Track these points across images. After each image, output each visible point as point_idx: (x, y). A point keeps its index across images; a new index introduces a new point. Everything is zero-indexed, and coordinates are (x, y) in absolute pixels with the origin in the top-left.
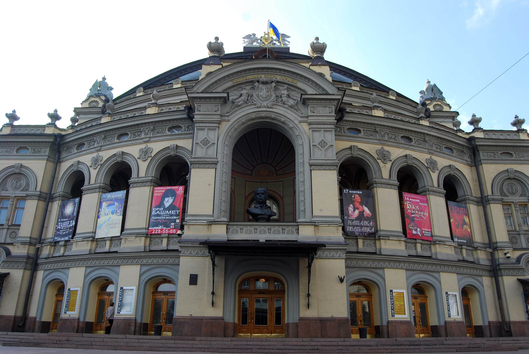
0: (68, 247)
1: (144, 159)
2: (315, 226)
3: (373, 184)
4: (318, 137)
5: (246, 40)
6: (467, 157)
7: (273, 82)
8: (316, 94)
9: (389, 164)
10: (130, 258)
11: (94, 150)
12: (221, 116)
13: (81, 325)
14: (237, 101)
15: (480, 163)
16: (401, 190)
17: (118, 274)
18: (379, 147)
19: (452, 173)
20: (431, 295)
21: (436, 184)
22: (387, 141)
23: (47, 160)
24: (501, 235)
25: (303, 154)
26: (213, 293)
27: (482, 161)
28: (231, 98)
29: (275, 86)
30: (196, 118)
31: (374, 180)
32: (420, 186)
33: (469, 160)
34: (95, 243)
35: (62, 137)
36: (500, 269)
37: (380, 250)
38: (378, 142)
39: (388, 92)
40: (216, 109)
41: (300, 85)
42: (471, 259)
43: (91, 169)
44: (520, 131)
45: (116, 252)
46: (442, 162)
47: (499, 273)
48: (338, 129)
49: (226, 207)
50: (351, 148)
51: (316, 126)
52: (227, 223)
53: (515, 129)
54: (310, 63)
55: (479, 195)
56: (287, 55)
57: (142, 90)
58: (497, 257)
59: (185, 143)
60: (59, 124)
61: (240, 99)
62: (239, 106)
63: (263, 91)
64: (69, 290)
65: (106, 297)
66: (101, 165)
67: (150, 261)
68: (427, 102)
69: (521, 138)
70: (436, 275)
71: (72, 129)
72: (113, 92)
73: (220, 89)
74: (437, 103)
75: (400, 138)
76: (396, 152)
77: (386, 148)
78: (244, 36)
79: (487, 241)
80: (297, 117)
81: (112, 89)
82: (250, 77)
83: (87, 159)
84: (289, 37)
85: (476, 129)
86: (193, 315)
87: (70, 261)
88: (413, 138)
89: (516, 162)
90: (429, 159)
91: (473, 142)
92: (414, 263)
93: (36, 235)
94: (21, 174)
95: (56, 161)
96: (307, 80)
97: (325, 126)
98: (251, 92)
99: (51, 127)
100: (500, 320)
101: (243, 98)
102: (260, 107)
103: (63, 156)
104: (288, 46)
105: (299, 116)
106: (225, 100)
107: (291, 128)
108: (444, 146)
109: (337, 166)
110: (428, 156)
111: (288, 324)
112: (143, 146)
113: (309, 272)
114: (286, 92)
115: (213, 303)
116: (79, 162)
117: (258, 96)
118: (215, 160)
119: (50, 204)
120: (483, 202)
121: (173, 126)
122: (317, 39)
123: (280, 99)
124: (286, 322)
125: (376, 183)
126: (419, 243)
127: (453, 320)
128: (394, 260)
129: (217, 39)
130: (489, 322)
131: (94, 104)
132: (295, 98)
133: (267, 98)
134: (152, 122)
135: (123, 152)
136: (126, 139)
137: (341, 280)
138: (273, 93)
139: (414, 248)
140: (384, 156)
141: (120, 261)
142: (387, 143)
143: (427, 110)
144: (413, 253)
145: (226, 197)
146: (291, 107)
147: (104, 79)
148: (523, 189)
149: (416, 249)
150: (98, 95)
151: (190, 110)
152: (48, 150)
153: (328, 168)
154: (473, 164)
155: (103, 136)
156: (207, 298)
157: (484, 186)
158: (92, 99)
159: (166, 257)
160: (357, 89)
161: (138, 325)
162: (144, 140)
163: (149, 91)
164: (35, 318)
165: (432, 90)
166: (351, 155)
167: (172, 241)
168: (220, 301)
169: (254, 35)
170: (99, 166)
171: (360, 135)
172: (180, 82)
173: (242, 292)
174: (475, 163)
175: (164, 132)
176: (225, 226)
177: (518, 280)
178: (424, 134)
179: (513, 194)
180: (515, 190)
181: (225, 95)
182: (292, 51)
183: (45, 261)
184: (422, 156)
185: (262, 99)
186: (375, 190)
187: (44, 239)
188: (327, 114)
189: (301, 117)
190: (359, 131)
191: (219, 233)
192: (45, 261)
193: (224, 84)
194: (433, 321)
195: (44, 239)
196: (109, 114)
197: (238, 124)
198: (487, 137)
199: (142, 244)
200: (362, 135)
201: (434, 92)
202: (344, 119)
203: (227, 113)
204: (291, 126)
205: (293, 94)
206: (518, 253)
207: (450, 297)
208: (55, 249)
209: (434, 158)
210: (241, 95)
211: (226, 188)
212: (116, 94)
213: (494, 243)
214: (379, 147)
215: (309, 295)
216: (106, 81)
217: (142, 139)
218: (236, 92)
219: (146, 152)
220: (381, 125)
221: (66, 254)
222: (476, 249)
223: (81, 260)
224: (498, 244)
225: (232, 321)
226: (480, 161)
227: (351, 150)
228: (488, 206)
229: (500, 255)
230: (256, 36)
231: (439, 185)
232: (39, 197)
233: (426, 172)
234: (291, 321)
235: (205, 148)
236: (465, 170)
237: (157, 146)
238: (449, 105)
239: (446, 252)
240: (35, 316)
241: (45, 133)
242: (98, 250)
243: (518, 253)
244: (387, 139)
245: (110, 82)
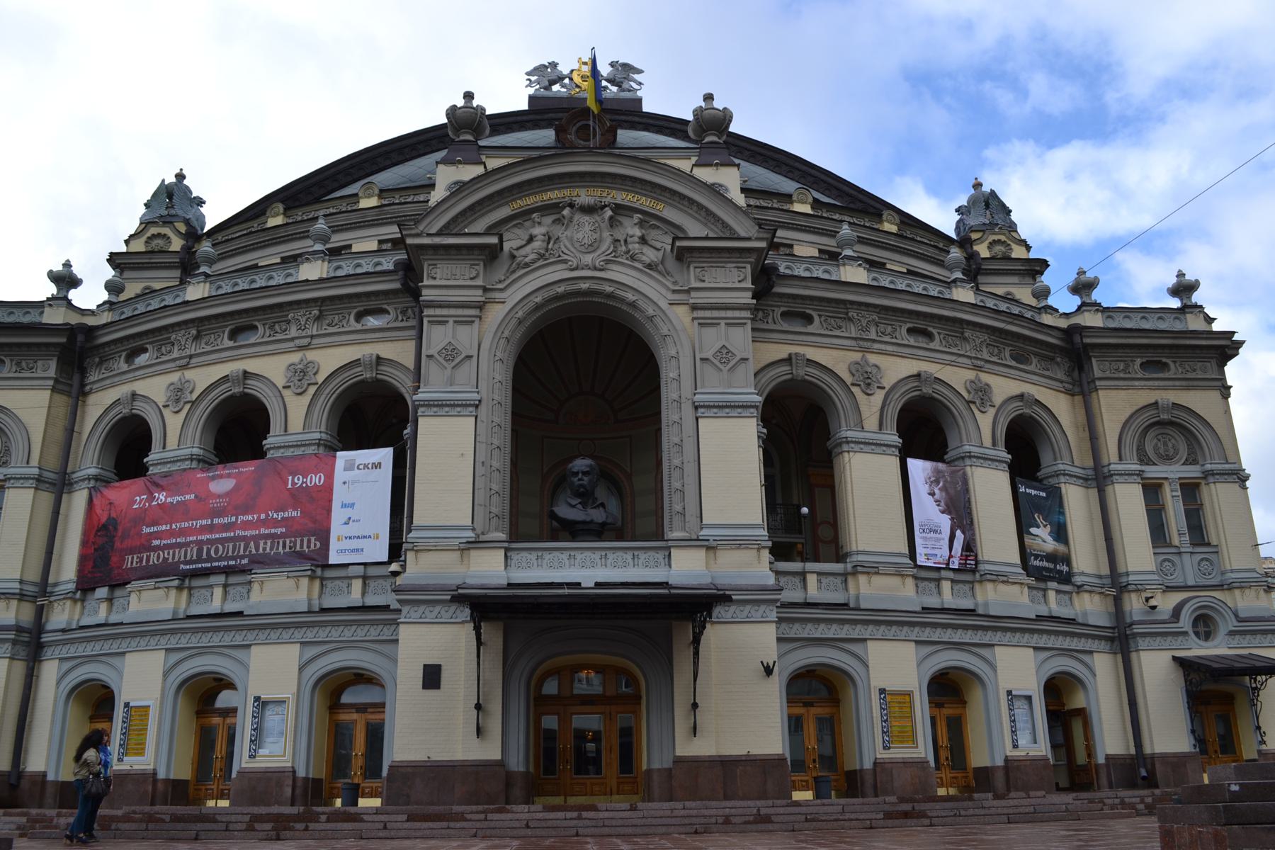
0: (116, 603)
1: (300, 391)
2: (708, 548)
3: (840, 444)
4: (712, 340)
5: (533, 78)
6: (1060, 375)
7: (605, 206)
8: (707, 238)
9: (879, 397)
10: (274, 627)
11: (172, 365)
12: (485, 290)
13: (160, 786)
14: (522, 252)
15: (1092, 386)
16: (905, 453)
17: (246, 667)
18: (857, 356)
19: (1027, 411)
20: (976, 698)
21: (987, 441)
22: (874, 341)
23: (54, 390)
24: (1138, 554)
25: (678, 380)
26: (478, 707)
27: (1098, 383)
28: (506, 246)
29: (611, 218)
30: (427, 294)
31: (843, 434)
32: (952, 443)
33: (1069, 380)
34: (185, 593)
35: (91, 331)
36: (1135, 635)
37: (857, 598)
38: (853, 343)
39: (880, 216)
40: (474, 274)
42: (1065, 612)
43: (166, 412)
45: (239, 614)
46: (1004, 387)
47: (1132, 644)
48: (760, 315)
49: (500, 505)
50: (788, 360)
51: (708, 314)
52: (506, 545)
53: (1175, 303)
54: (694, 159)
55: (1090, 463)
56: (637, 119)
57: (282, 210)
58: (1127, 608)
59: (400, 351)
60: (76, 296)
61: (528, 249)
62: (527, 265)
63: (584, 229)
64: (127, 705)
65: (216, 720)
66: (193, 403)
67: (322, 634)
68: (974, 236)
69: (1191, 328)
70: (984, 652)
71: (110, 310)
72: (204, 210)
73: (480, 226)
74: (996, 238)
75: (904, 331)
76: (896, 369)
77: (873, 359)
78: (530, 68)
79: (1105, 571)
80: (663, 291)
81: (201, 202)
82: (553, 195)
83: (155, 388)
84: (640, 72)
86: (433, 758)
87: (124, 636)
88: (935, 331)
89: (1177, 383)
90: (972, 382)
91: (1077, 339)
92: (935, 625)
93: (34, 575)
95: (75, 390)
96: (686, 203)
97: (730, 314)
98: (558, 231)
99: (59, 306)
100: (1133, 751)
101: (537, 244)
102: (576, 269)
103: (92, 379)
104: (639, 94)
105: (668, 289)
106: (491, 255)
107: (651, 318)
108: (1008, 349)
109: (756, 407)
110: (971, 375)
111: (649, 771)
112: (295, 358)
113: (696, 654)
115: (479, 731)
116: (134, 395)
117: (571, 240)
118: (475, 396)
119: (65, 496)
120: (1099, 479)
121: (368, 305)
122: (709, 97)
123: (624, 248)
124: (644, 767)
125: (848, 442)
126: (947, 579)
127: (1023, 754)
128: (888, 620)
129: (469, 96)
130: (1108, 757)
131: (159, 243)
132: (659, 245)
133: (592, 247)
134: (315, 300)
135: (245, 372)
136: (252, 340)
137: (768, 671)
138: (606, 234)
139: (935, 591)
140: (868, 380)
141: (251, 637)
142: (876, 346)
143: (972, 256)
144: (933, 602)
145: (500, 483)
146: (649, 266)
147: (180, 177)
148: (1190, 447)
149: (939, 593)
150: (167, 221)
151: (410, 273)
152: (53, 364)
153: (735, 412)
154: (1077, 389)
155: (194, 332)
156: (464, 716)
157: (1102, 440)
158: (153, 230)
159: (360, 623)
160: (806, 209)
161: (299, 784)
162: (298, 342)
163: (299, 215)
164: (44, 774)
165: (987, 206)
166: (789, 377)
167: (372, 584)
169: (554, 65)
170: (187, 407)
171: (810, 329)
172: (377, 192)
173: (539, 704)
174: (1081, 387)
175: (344, 322)
176: (502, 552)
177: (1174, 658)
178: (962, 321)
179: (1167, 459)
180: (1171, 452)
181: (494, 240)
182: (647, 108)
183: (60, 637)
185: (583, 249)
186: (847, 459)
187: (55, 585)
188: (734, 284)
189: (674, 291)
190: (809, 319)
191: (490, 569)
192: (60, 637)
193: (490, 211)
194: (979, 757)
195: (55, 585)
196: (207, 275)
197: (526, 308)
198: (1112, 324)
199: (302, 595)
200: (815, 327)
201: (988, 210)
202: (777, 290)
203: (500, 282)
204: (651, 312)
205: (653, 235)
206: (1177, 597)
207: (1017, 703)
208: (83, 608)
209: (985, 378)
210: (531, 239)
211: (501, 461)
212: (213, 215)
213: (1120, 575)
215: (695, 706)
216: (185, 182)
217: (292, 339)
218: (516, 231)
219: (304, 372)
220: (860, 304)
221: (114, 618)
222: (1080, 588)
223: (153, 633)
224: (1131, 578)
225: (522, 769)
226: (1093, 381)
227: (791, 365)
228: (1109, 489)
229: (1134, 605)
230: (559, 68)
231: (994, 444)
232: (38, 480)
233: (965, 413)
234: (656, 765)
235: (449, 366)
236: (1061, 406)
237: (329, 359)
238: (1024, 241)
239: (1011, 598)
240: (42, 769)
241: (44, 321)
242: (195, 610)
243: (1177, 597)
244: (873, 336)
245: (196, 186)
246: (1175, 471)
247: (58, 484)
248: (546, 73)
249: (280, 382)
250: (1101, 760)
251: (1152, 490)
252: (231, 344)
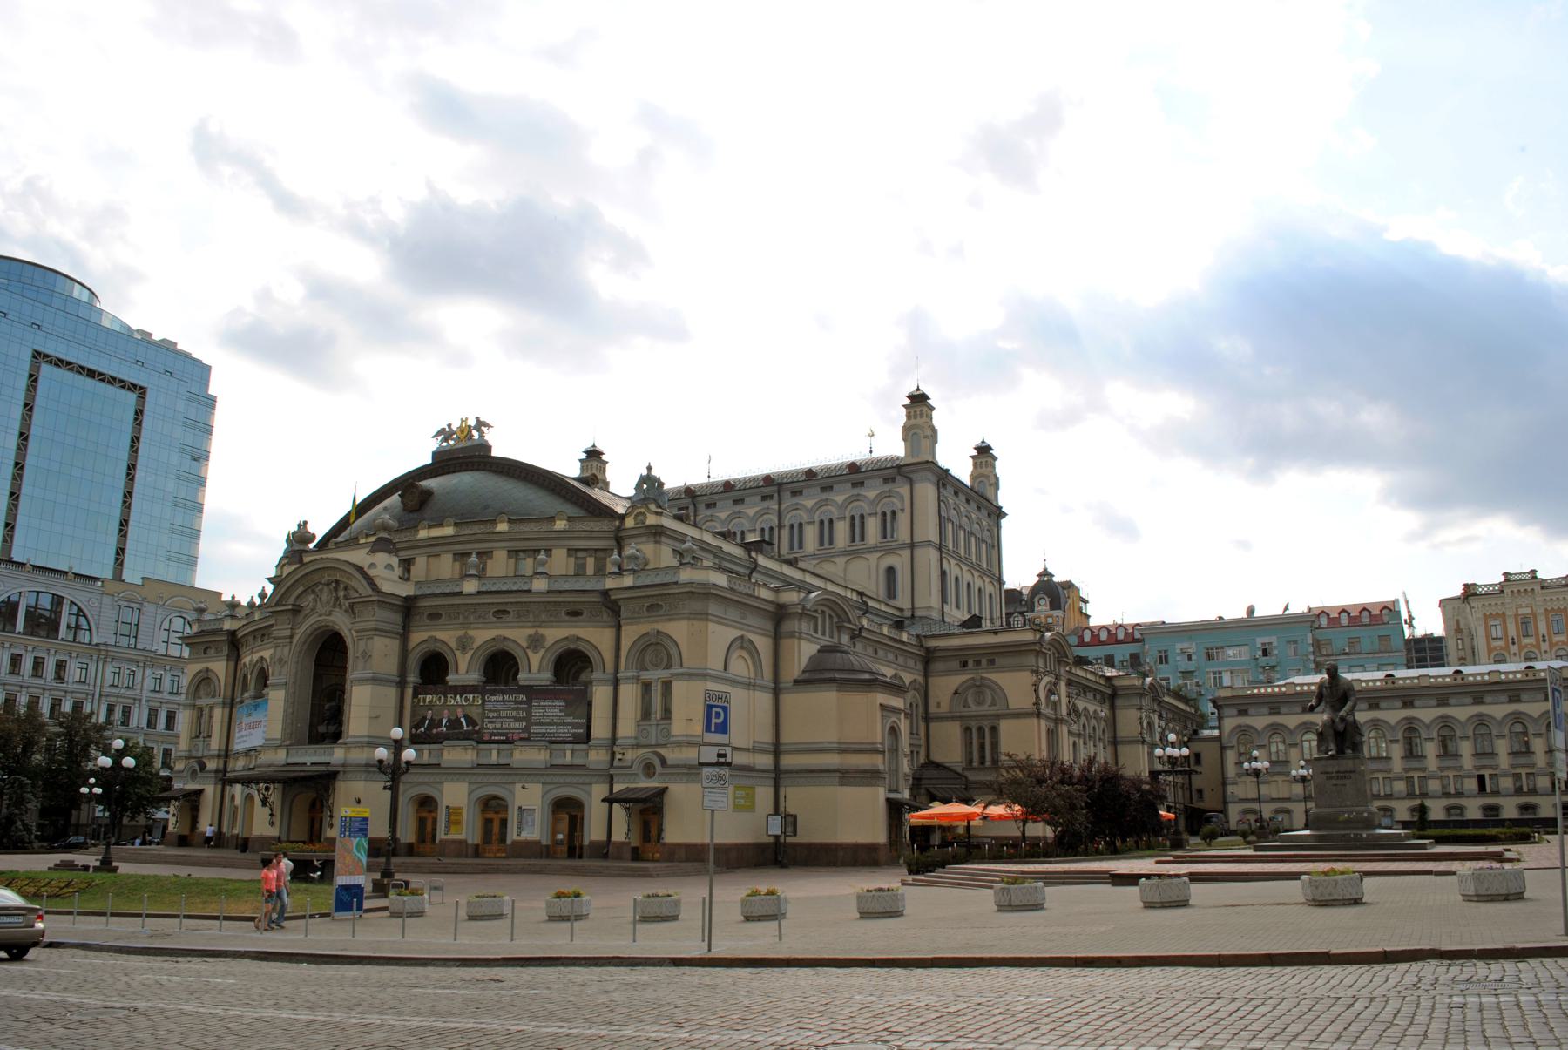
6: (605, 617)
9: (470, 654)
18: (462, 633)
19: (572, 646)
76: (483, 636)
77: (471, 633)
115: (272, 824)
128: (457, 773)
140: (464, 645)
168: (277, 820)
179: (656, 666)
191: (281, 757)
209: (541, 631)
214: (462, 633)
246: (655, 675)
247: (231, 704)
250: (586, 843)
251: (647, 687)
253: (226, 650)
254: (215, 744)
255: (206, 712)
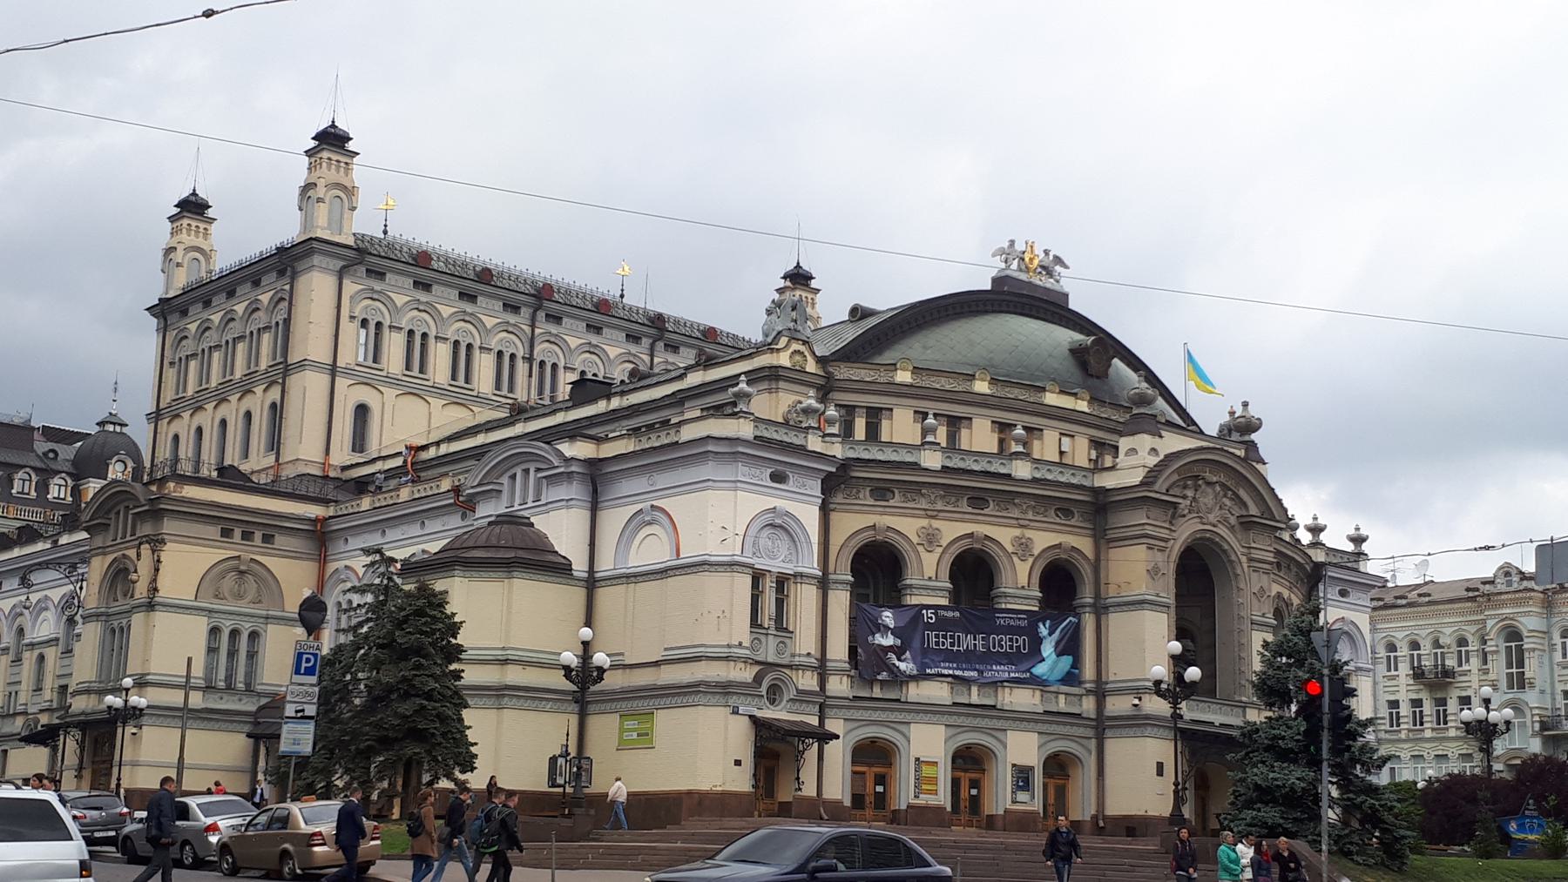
41: (1242, 493)
43: (920, 548)
44: (1360, 555)
59: (1084, 544)
63: (1207, 498)
82: (1196, 470)
84: (1066, 267)
85: (1316, 544)
94: (781, 527)
112: (1017, 532)
114: (1228, 502)
121: (1065, 509)
169: (1012, 243)
170: (940, 550)
183: (846, 703)
184: (1286, 594)
248: (1007, 253)
249: (1010, 549)
252: (970, 510)
253: (815, 487)
254: (805, 642)
255: (769, 585)
